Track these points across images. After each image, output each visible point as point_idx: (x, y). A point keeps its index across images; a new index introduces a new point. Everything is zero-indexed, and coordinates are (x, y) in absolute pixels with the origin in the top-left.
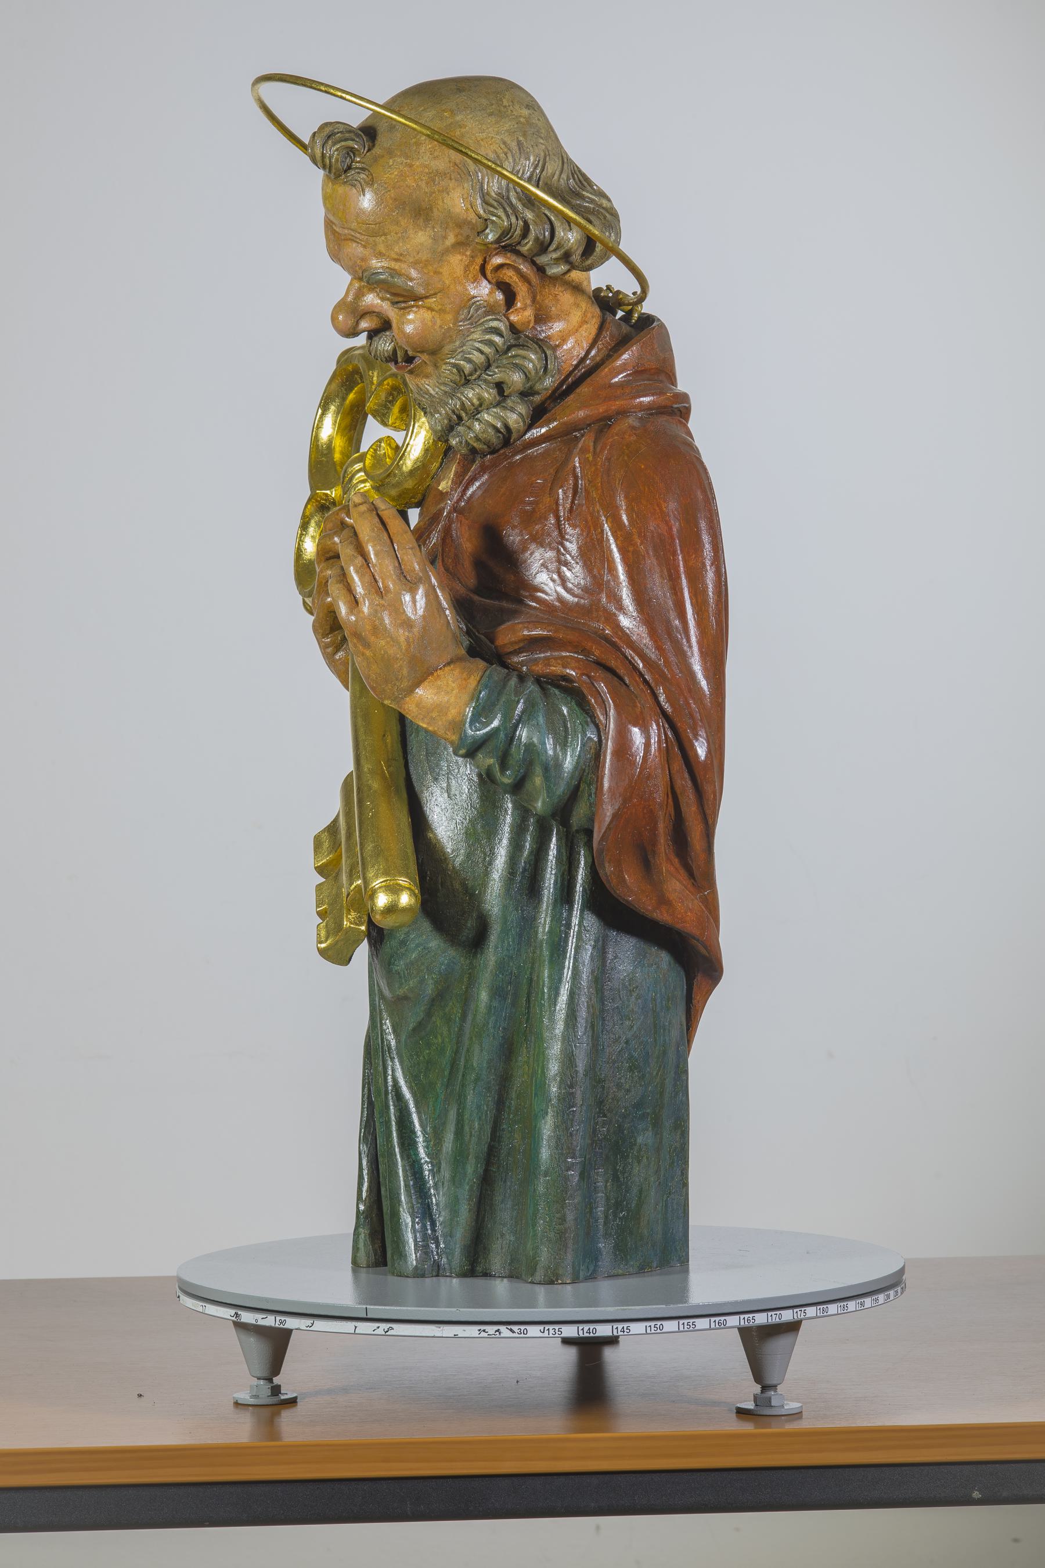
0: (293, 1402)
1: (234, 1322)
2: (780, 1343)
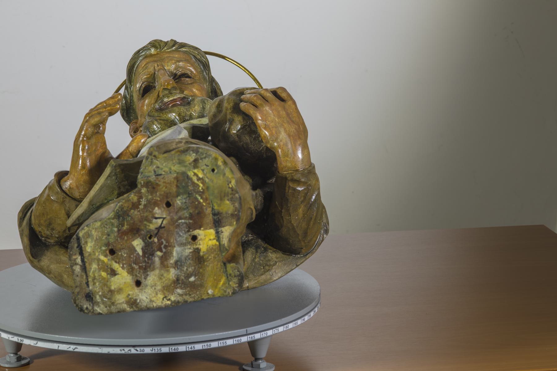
0: (28, 364)
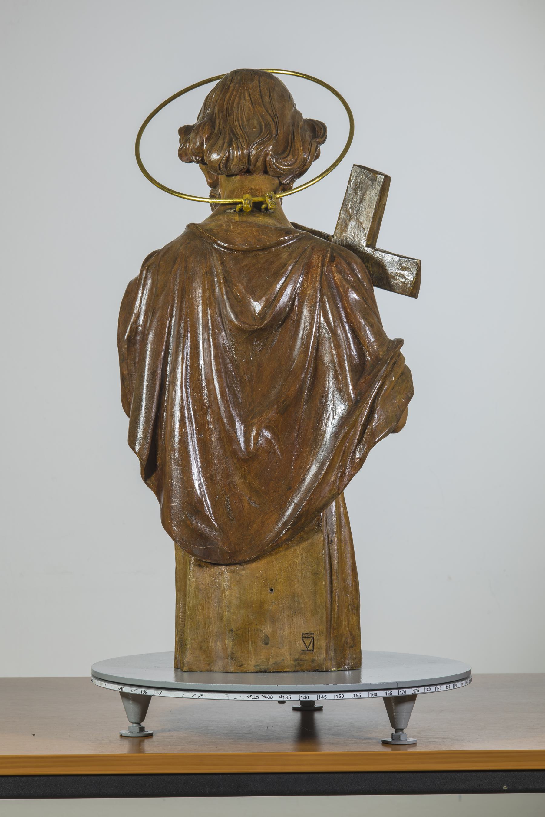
0: (150, 735)
1: (120, 692)
2: (405, 707)
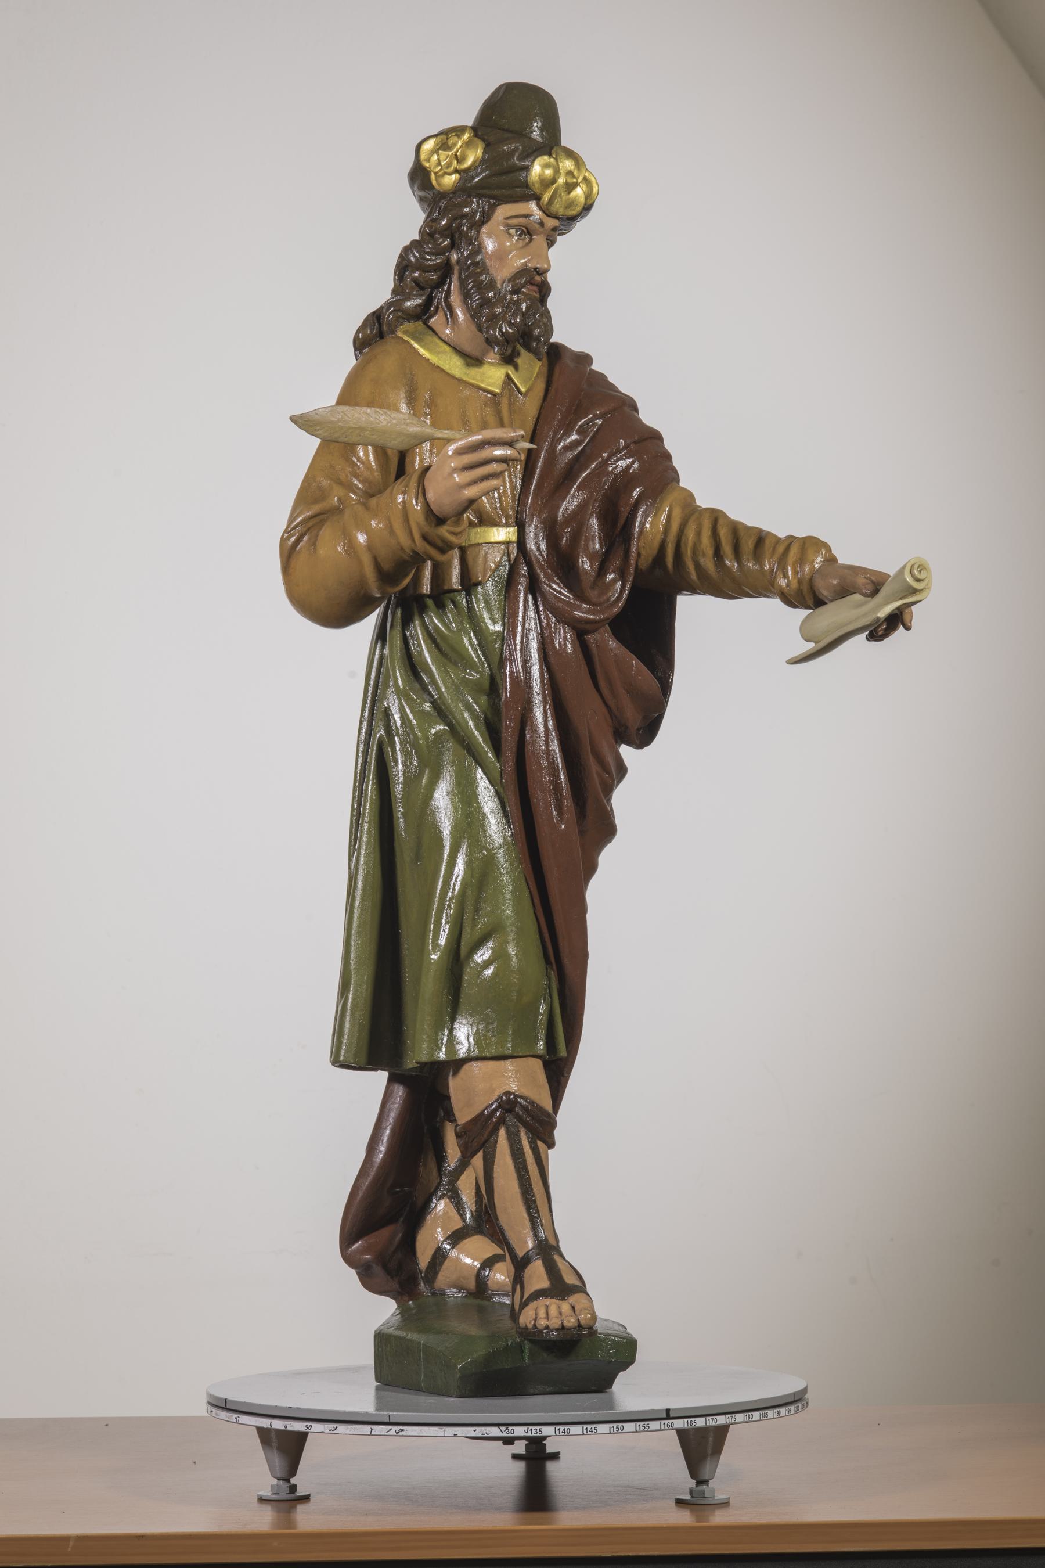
0: (306, 1498)
1: (261, 1431)
